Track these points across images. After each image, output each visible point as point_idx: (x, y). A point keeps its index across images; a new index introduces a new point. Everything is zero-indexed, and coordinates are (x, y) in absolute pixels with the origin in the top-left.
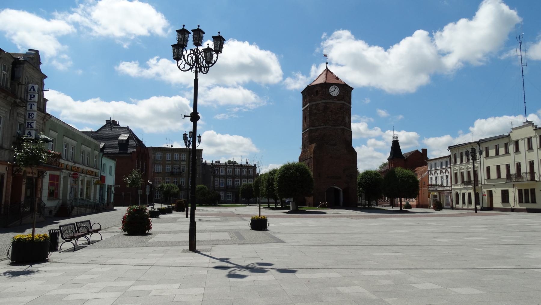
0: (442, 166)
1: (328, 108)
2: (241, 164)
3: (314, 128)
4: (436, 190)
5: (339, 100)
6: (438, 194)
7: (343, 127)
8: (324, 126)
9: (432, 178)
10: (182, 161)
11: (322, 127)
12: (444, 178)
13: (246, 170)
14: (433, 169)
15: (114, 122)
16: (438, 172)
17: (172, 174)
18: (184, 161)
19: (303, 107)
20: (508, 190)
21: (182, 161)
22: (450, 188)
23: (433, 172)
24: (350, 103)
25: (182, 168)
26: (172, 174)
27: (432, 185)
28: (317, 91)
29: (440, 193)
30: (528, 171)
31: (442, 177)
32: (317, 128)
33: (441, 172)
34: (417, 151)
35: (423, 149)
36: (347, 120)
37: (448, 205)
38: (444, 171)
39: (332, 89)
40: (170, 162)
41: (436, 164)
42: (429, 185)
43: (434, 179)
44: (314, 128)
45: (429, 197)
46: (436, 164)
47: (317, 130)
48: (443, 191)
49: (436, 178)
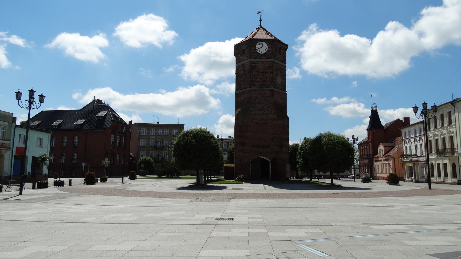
0: (415, 134)
1: (262, 70)
2: (222, 138)
4: (411, 161)
5: (267, 58)
6: (412, 165)
7: (272, 88)
8: (250, 89)
9: (406, 147)
10: (165, 135)
11: (247, 89)
12: (419, 147)
13: (227, 143)
14: (407, 137)
15: (99, 101)
16: (412, 140)
17: (155, 148)
18: (167, 135)
20: (17, 147)
21: (165, 135)
22: (424, 159)
23: (407, 141)
25: (165, 142)
26: (155, 148)
27: (407, 156)
28: (244, 50)
29: (414, 164)
31: (416, 146)
32: (243, 91)
33: (415, 140)
35: (404, 118)
36: (279, 80)
37: (423, 177)
38: (418, 139)
39: (259, 45)
40: (154, 137)
41: (410, 132)
42: (404, 155)
43: (408, 148)
45: (404, 168)
46: (410, 132)
48: (417, 161)
49: (410, 147)
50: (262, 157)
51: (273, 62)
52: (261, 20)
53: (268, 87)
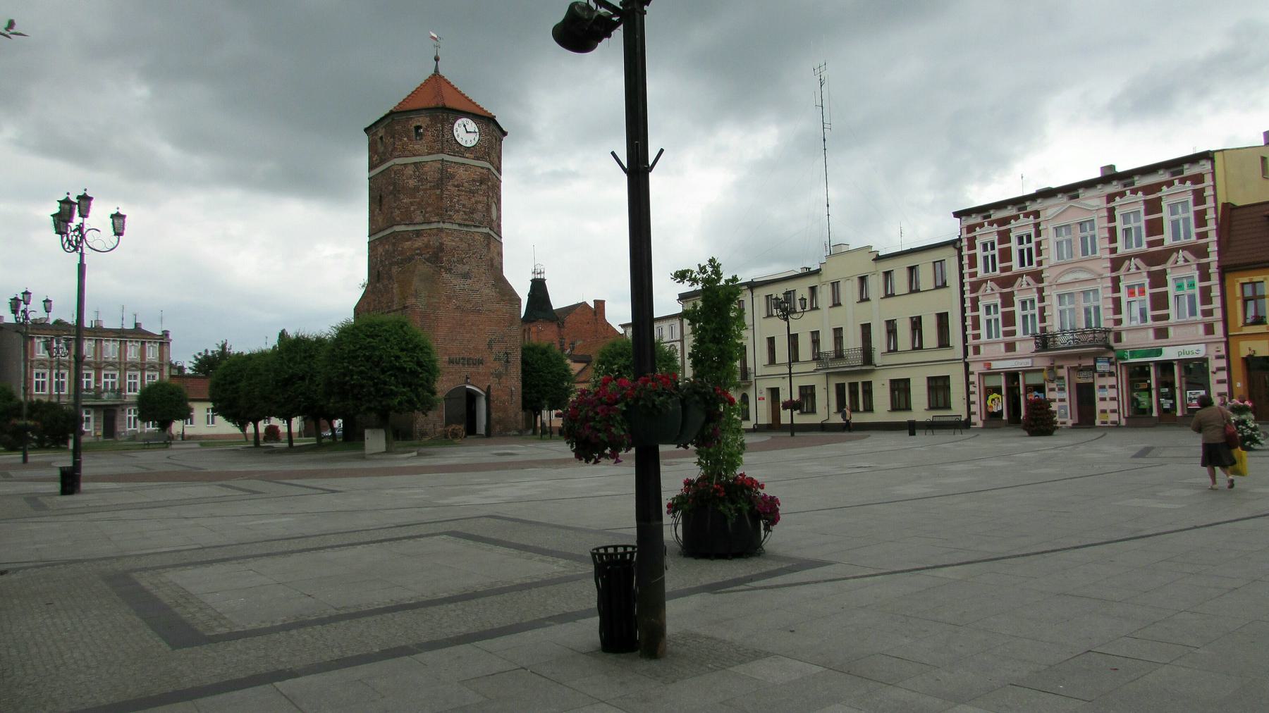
3: (411, 228)
7: (487, 230)
11: (434, 226)
19: (371, 168)
28: (418, 128)
30: (859, 345)
34: (584, 305)
44: (411, 228)
52: (437, 59)
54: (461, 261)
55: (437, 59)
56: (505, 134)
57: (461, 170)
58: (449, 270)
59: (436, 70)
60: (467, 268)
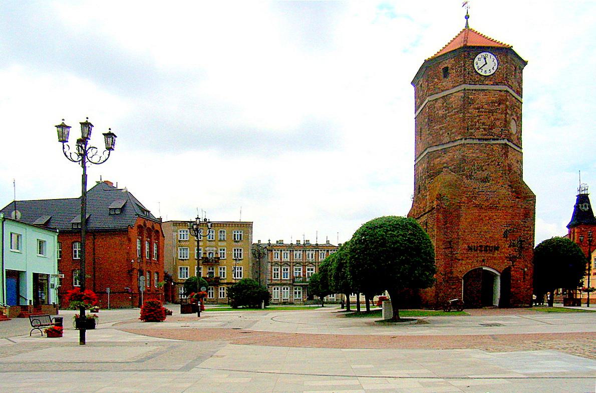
7: (505, 141)
8: (463, 141)
24: (520, 93)
28: (446, 70)
32: (445, 147)
36: (513, 128)
39: (479, 61)
47: (445, 151)
50: (484, 268)
51: (507, 91)
52: (467, 17)
53: (497, 139)
54: (481, 168)
55: (467, 17)
56: (525, 63)
57: (481, 96)
58: (469, 177)
59: (467, 26)
60: (485, 174)
